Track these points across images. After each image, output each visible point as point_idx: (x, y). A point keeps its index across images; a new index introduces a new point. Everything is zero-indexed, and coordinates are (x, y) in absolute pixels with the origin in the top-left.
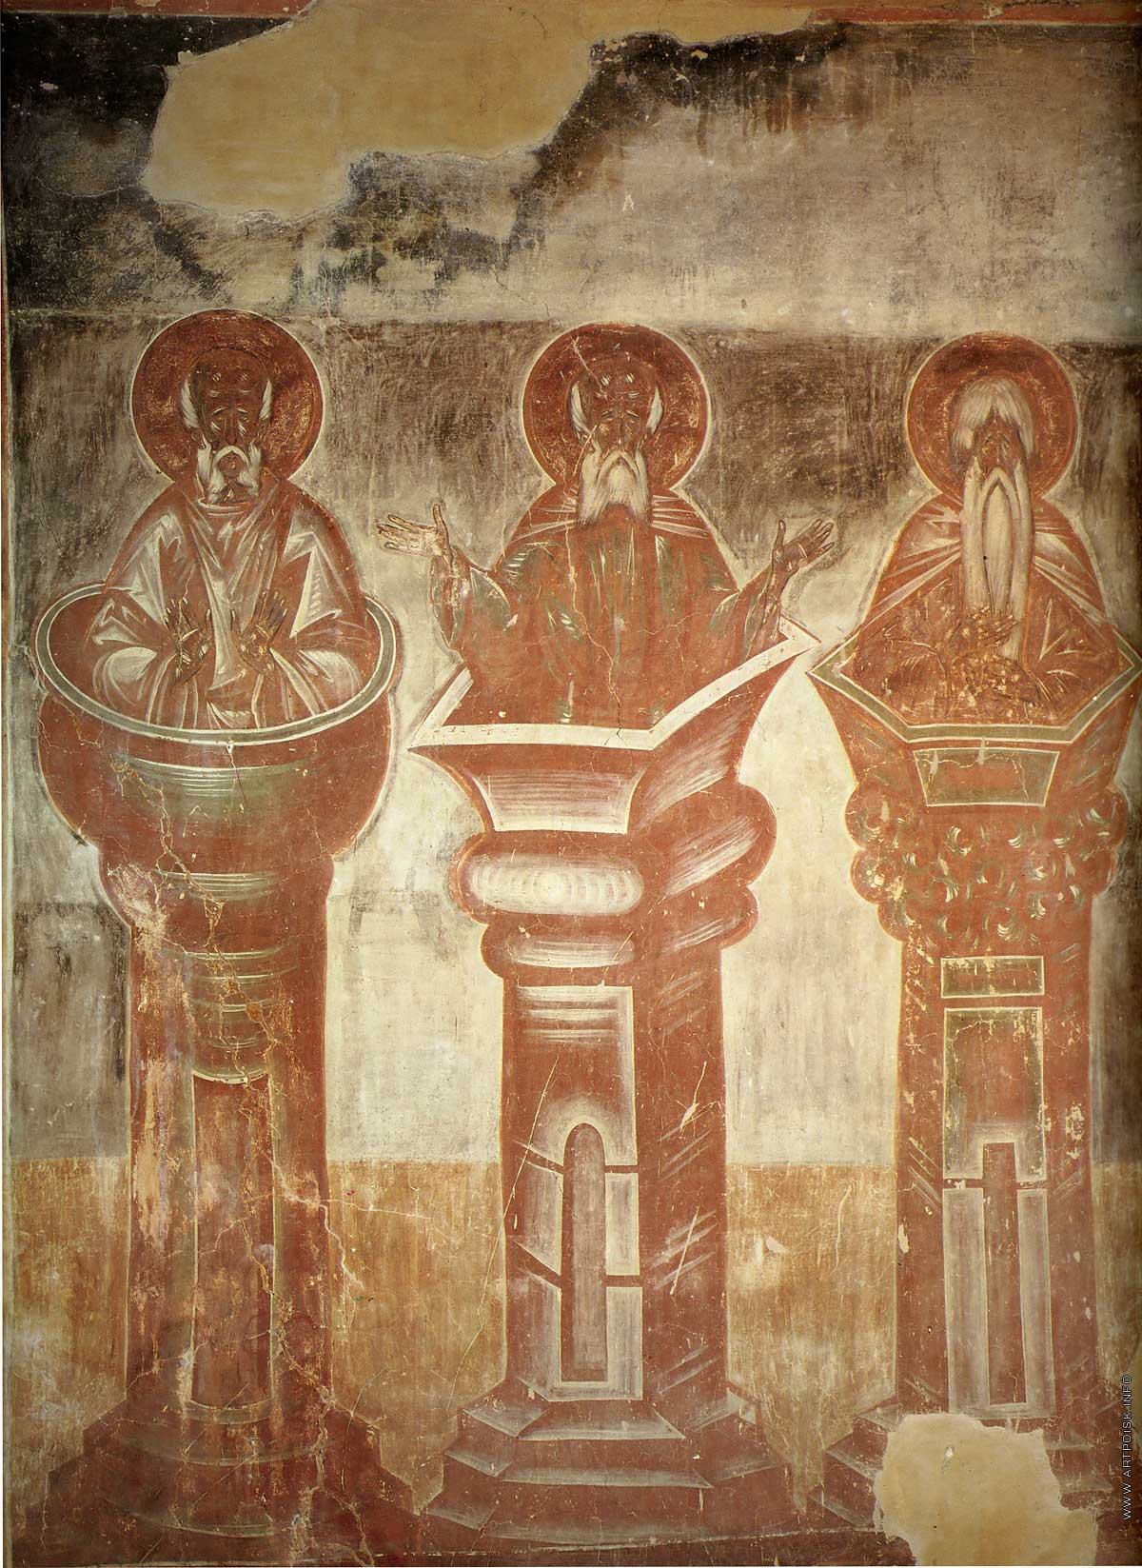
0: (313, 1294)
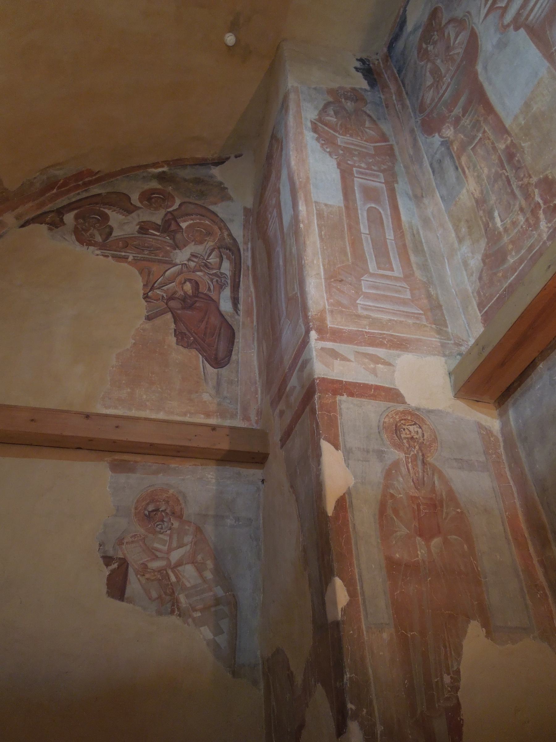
0: (519, 161)
